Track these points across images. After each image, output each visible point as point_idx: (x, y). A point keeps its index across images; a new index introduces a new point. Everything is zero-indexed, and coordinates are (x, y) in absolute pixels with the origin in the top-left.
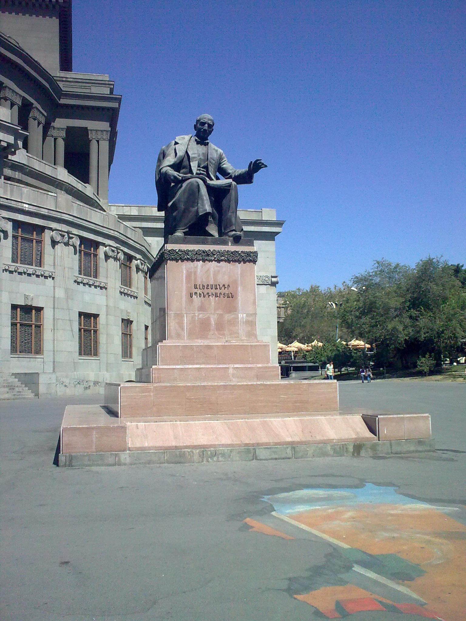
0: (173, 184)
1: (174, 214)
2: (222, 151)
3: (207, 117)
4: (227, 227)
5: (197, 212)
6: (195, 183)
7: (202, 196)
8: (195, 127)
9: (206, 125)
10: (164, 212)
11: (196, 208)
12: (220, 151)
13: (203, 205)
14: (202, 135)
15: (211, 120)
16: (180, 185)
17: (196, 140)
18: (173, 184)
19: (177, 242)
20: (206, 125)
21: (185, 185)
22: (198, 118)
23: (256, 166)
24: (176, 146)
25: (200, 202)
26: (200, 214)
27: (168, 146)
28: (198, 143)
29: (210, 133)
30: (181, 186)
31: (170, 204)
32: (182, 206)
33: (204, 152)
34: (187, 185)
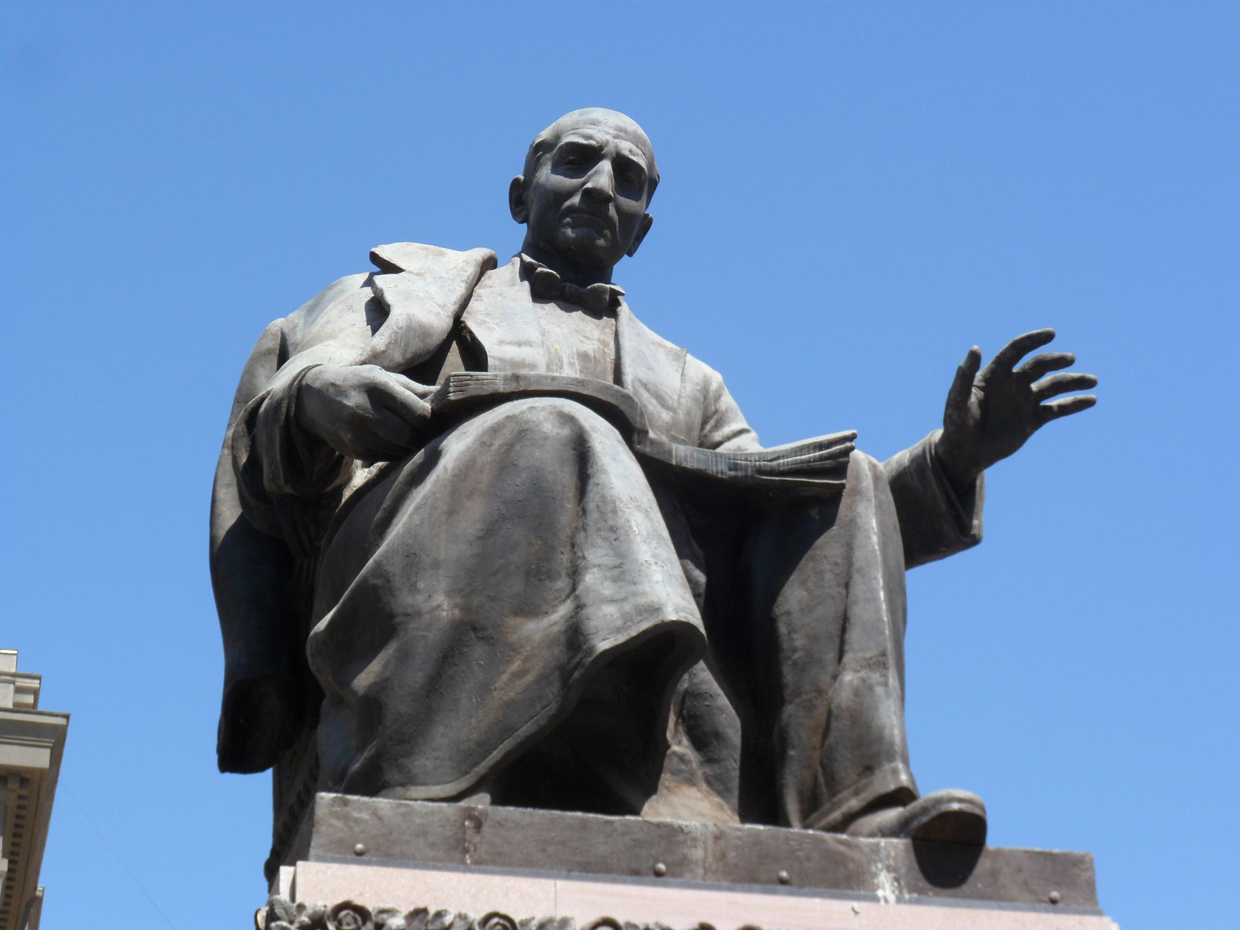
1: (363, 680)
2: (716, 378)
3: (605, 125)
5: (575, 635)
6: (550, 427)
7: (610, 508)
8: (520, 196)
9: (606, 166)
10: (269, 774)
11: (563, 610)
12: (699, 369)
13: (623, 570)
14: (577, 237)
15: (636, 140)
16: (419, 457)
17: (527, 272)
19: (383, 850)
20: (606, 166)
21: (458, 444)
22: (545, 134)
23: (1004, 404)
25: (596, 555)
26: (603, 645)
28: (542, 292)
29: (634, 231)
30: (433, 459)
32: (434, 603)
33: (590, 347)
34: (483, 443)
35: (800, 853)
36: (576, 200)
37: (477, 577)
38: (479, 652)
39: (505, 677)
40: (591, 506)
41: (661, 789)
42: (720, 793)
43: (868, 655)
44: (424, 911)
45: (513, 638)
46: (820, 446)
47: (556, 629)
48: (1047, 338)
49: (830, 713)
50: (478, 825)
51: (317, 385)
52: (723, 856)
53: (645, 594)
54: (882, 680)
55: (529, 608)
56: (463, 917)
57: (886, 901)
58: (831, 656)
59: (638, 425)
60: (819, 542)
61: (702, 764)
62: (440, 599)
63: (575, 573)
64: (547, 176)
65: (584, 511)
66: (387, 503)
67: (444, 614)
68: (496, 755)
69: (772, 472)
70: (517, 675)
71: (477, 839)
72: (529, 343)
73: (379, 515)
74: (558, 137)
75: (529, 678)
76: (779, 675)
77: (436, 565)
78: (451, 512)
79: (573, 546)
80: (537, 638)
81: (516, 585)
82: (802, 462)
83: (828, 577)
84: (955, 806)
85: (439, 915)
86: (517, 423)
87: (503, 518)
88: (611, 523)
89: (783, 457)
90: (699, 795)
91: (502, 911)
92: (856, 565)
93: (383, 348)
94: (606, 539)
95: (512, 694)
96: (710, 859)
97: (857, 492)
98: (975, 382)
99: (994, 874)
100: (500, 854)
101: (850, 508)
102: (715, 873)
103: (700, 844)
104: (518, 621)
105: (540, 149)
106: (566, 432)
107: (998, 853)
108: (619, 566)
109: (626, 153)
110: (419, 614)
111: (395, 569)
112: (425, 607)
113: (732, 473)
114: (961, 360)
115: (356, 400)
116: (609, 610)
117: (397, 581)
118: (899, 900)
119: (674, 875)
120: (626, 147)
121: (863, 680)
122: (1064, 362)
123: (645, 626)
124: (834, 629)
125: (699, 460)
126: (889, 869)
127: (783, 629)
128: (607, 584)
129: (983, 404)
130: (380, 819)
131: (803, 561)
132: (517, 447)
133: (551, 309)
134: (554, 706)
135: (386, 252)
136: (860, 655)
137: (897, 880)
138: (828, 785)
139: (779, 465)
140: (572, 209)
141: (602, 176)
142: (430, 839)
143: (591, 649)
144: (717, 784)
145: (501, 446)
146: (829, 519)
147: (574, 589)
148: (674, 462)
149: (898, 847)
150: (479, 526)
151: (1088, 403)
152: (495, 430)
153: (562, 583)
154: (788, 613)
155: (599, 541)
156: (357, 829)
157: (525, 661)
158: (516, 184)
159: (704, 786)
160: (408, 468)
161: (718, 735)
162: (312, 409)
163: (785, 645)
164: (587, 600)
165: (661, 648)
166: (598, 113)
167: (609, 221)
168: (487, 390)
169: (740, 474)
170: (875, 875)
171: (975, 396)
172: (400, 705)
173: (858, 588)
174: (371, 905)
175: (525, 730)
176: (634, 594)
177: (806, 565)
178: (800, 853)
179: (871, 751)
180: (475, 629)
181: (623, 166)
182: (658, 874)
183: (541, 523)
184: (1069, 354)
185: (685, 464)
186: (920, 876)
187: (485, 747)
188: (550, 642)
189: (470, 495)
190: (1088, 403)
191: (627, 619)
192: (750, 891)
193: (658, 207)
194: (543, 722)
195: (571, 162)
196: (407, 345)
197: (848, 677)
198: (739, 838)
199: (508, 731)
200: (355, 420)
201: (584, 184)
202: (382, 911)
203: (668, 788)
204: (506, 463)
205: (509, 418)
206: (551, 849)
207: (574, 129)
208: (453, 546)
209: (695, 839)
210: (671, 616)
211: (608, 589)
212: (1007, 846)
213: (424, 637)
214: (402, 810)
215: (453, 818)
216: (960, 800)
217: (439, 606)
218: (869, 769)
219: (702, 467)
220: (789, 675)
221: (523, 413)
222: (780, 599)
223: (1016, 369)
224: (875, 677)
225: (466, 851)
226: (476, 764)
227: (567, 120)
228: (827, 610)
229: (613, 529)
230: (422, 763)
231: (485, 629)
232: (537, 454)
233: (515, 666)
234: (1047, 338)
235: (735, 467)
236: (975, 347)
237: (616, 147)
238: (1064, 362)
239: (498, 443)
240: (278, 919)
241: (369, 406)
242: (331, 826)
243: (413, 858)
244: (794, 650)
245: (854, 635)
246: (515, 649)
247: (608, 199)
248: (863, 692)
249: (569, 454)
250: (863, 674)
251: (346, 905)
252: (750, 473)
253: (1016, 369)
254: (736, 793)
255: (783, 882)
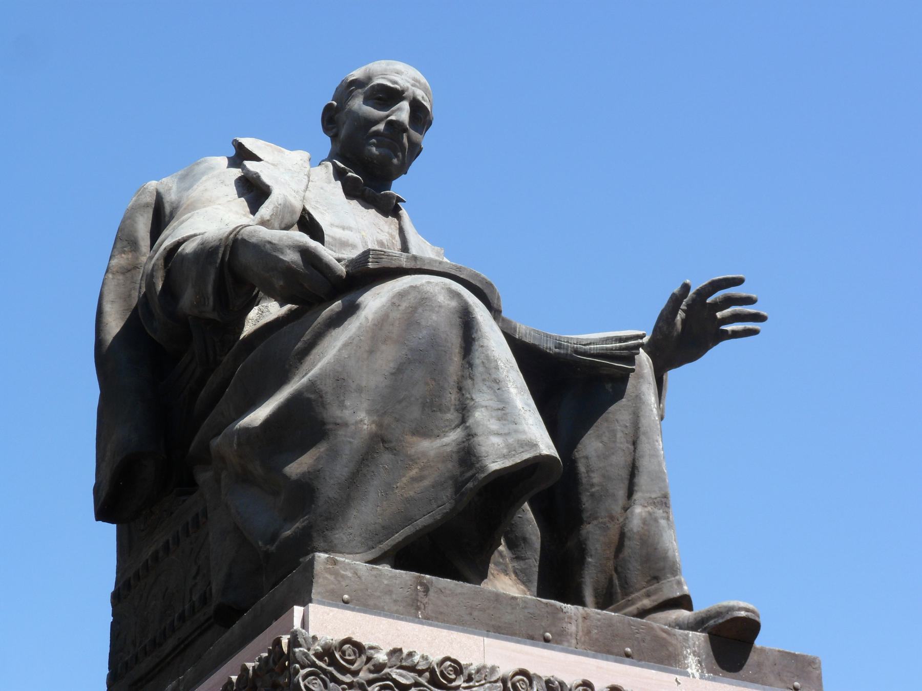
0: (267, 311)
1: (296, 468)
3: (401, 74)
4: (627, 588)
5: (467, 455)
6: (442, 298)
7: (490, 365)
9: (405, 105)
11: (453, 437)
16: (337, 305)
17: (339, 174)
18: (267, 311)
20: (405, 105)
21: (375, 301)
22: (357, 74)
24: (250, 165)
25: (482, 398)
26: (495, 465)
27: (188, 178)
30: (351, 309)
31: (259, 415)
32: (357, 416)
35: (637, 636)
36: (381, 127)
37: (389, 403)
38: (386, 458)
39: (404, 480)
40: (477, 362)
41: (490, 576)
42: (524, 583)
43: (653, 496)
44: (400, 650)
45: (411, 451)
46: (620, 339)
47: (449, 449)
48: (738, 282)
49: (622, 536)
50: (426, 591)
51: (253, 240)
52: (588, 633)
53: (524, 432)
54: (665, 515)
55: (423, 431)
56: (424, 658)
57: (694, 677)
58: (621, 493)
59: (495, 306)
60: (612, 408)
61: (512, 559)
62: (362, 415)
63: (464, 411)
64: (358, 104)
65: (471, 365)
66: (308, 336)
67: (365, 427)
68: (398, 537)
69: (585, 354)
70: (414, 480)
71: (425, 600)
72: (350, 229)
73: (300, 345)
74: (369, 79)
75: (426, 483)
76: (578, 502)
77: (360, 390)
78: (371, 352)
79: (460, 389)
80: (432, 453)
81: (415, 413)
82: (607, 349)
83: (619, 435)
84: (743, 614)
85: (411, 654)
86: (419, 292)
87: (410, 362)
88: (494, 376)
89: (594, 344)
90: (510, 582)
91: (453, 657)
92: (642, 429)
93: (268, 218)
94: (490, 387)
95: (412, 493)
96: (580, 633)
97: (640, 376)
98: (683, 307)
99: (759, 665)
100: (441, 613)
101: (636, 387)
102: (584, 643)
103: (573, 622)
104: (415, 439)
105: (357, 84)
106: (454, 304)
107: (762, 650)
108: (502, 409)
109: (420, 98)
110: (346, 425)
111: (327, 387)
112: (352, 420)
113: (557, 350)
114: (676, 289)
115: (291, 257)
116: (495, 440)
117: (329, 398)
118: (702, 677)
119: (557, 643)
120: (420, 94)
121: (650, 514)
122: (749, 301)
123: (527, 456)
124: (625, 474)
125: (534, 337)
126: (695, 654)
127: (582, 468)
128: (493, 421)
129: (684, 322)
130: (359, 577)
131: (599, 420)
132: (420, 310)
133: (355, 203)
134: (448, 507)
135: (250, 143)
136: (648, 495)
137: (700, 662)
138: (622, 587)
139: (590, 349)
140: (377, 134)
141: (402, 113)
142: (394, 596)
143: (483, 468)
144: (522, 576)
145: (407, 308)
146: (619, 394)
147: (463, 421)
148: (517, 337)
149: (698, 638)
150: (392, 365)
151: (754, 332)
152: (402, 295)
153: (452, 416)
154: (587, 458)
155: (484, 388)
156: (344, 584)
157: (422, 469)
158: (328, 109)
159: (513, 576)
160: (327, 312)
161: (525, 540)
162: (246, 258)
163: (584, 481)
164: (479, 431)
165: (526, 476)
166: (400, 66)
167: (402, 145)
168: (394, 264)
169: (562, 351)
170: (686, 657)
171: (680, 316)
172: (329, 490)
173: (644, 446)
174: (366, 643)
175: (422, 522)
176: (516, 431)
177: (601, 424)
178: (637, 636)
179: (658, 567)
180: (384, 441)
181: (417, 108)
182: (546, 640)
183: (438, 368)
184: (754, 296)
185: (524, 339)
186: (714, 661)
187: (389, 531)
188: (443, 458)
189: (385, 341)
190: (754, 332)
191: (512, 450)
192: (607, 660)
193: (427, 140)
194: (438, 517)
195: (379, 99)
196: (283, 218)
197: (638, 510)
198: (599, 620)
199: (410, 520)
200: (288, 271)
201: (388, 116)
202: (371, 648)
203: (493, 574)
204: (411, 321)
205: (413, 288)
206: (476, 613)
207: (383, 75)
208: (374, 375)
209: (570, 618)
210: (545, 452)
211: (494, 425)
212: (768, 646)
213: (350, 442)
214: (374, 572)
215: (410, 583)
216: (747, 610)
217: (361, 421)
218: (656, 579)
219: (537, 343)
220: (587, 502)
221: (423, 285)
222: (579, 446)
223: (709, 301)
224: (659, 512)
225: (418, 608)
226: (380, 542)
227: (377, 66)
228: (620, 460)
229: (497, 381)
230: (339, 536)
231: (390, 442)
232: (434, 317)
233: (414, 472)
234: (738, 282)
235: (559, 346)
236: (688, 281)
237: (414, 93)
238: (749, 301)
239: (404, 305)
240: (300, 646)
241: (301, 263)
242: (326, 578)
243: (383, 609)
244: (592, 485)
245: (642, 480)
246: (413, 460)
247: (405, 130)
248: (650, 521)
249: (457, 321)
250: (649, 509)
251: (348, 641)
252: (569, 352)
253: (709, 301)
254: (536, 584)
255: (628, 655)
